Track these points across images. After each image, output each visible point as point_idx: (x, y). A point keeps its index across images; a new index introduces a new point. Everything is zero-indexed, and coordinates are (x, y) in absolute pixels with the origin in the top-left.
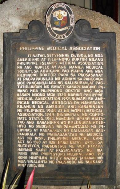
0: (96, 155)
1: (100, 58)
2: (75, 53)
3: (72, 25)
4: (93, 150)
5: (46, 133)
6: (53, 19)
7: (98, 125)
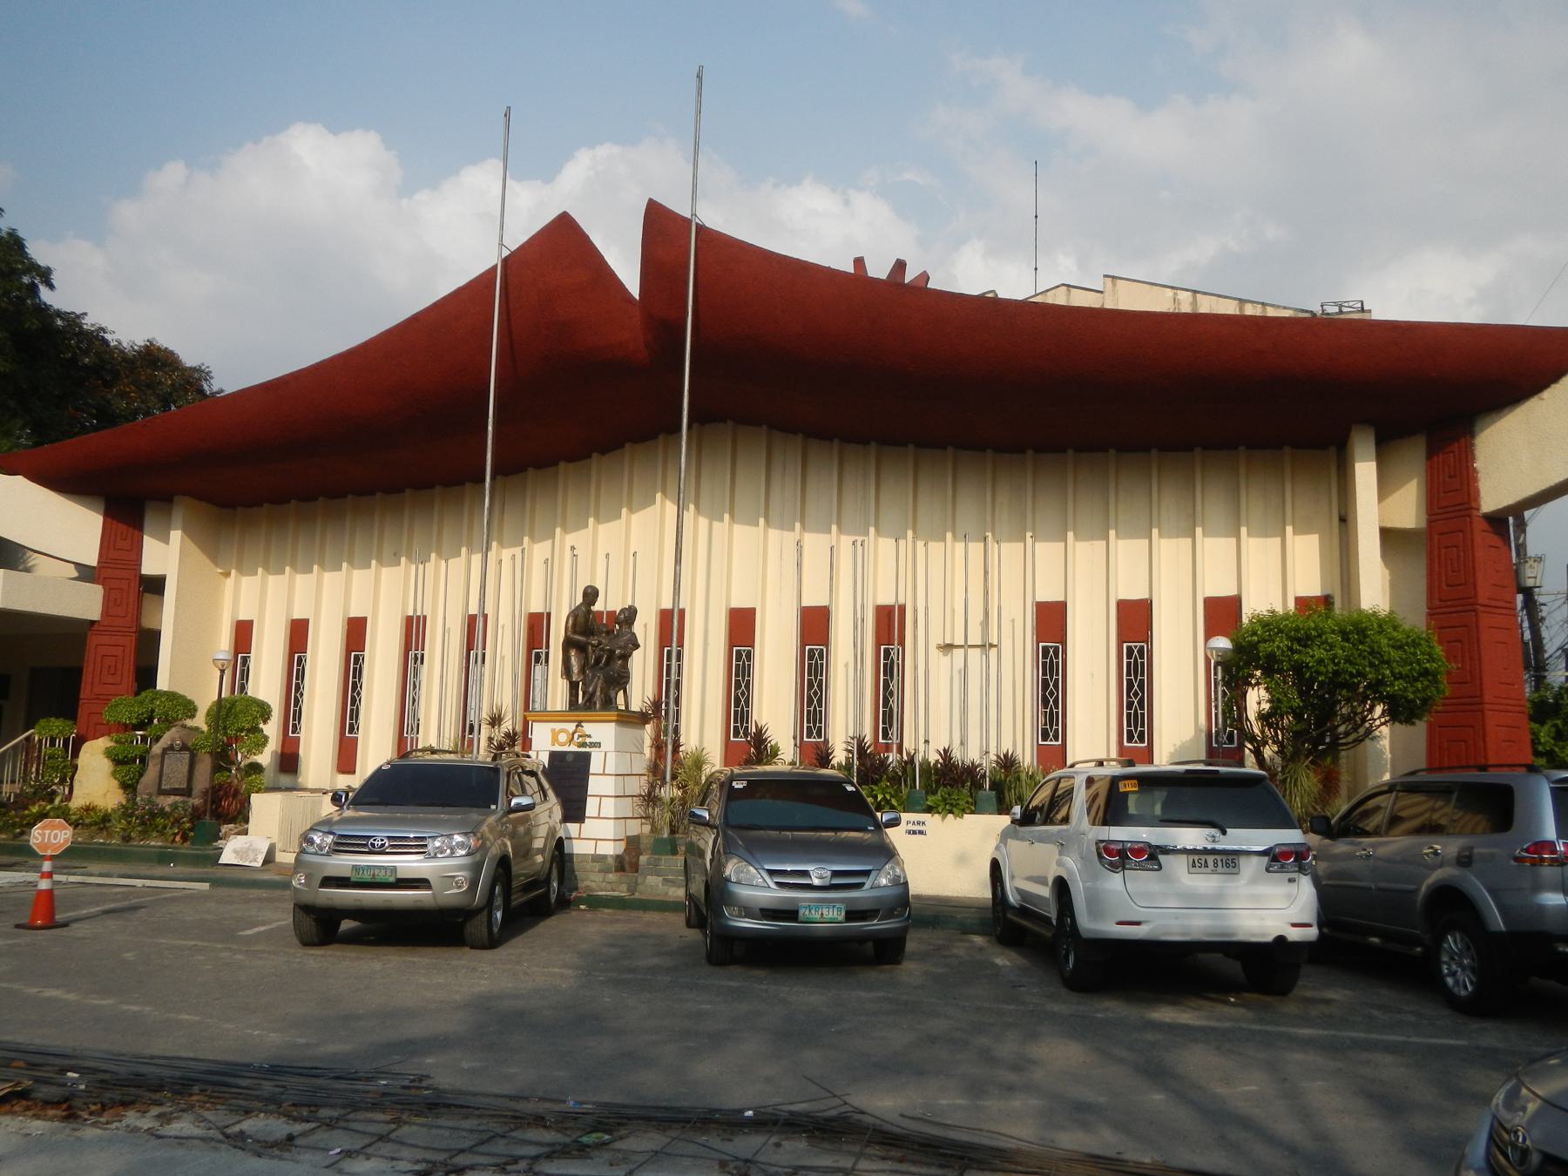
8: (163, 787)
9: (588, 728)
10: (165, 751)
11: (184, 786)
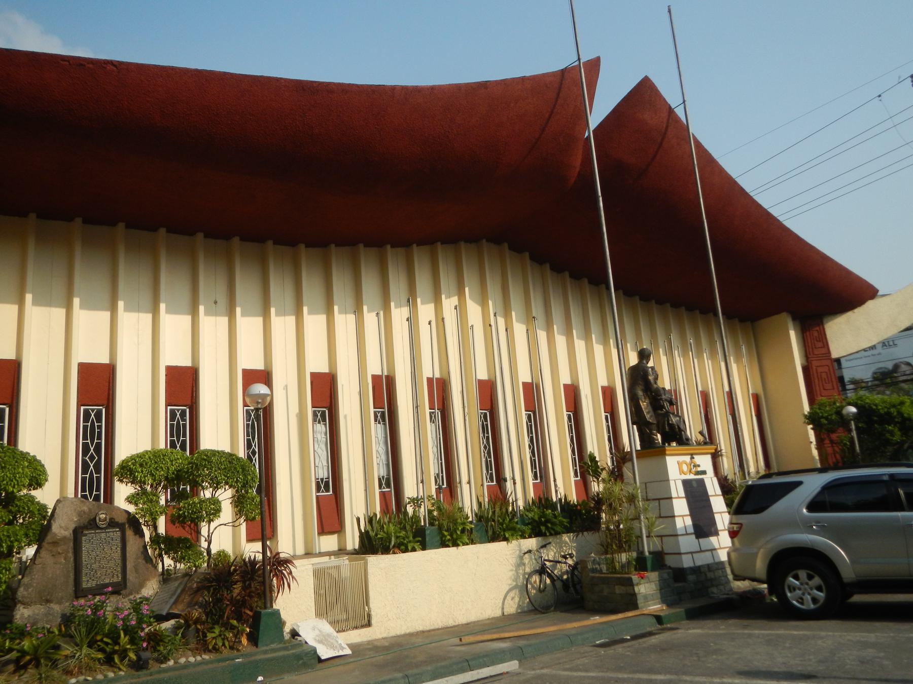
0: (118, 577)
1: (119, 533)
2: (108, 532)
3: (108, 520)
4: (117, 575)
5: (96, 570)
6: (100, 518)
7: (118, 564)
8: (84, 585)
9: (698, 459)
10: (78, 533)
11: (118, 579)
